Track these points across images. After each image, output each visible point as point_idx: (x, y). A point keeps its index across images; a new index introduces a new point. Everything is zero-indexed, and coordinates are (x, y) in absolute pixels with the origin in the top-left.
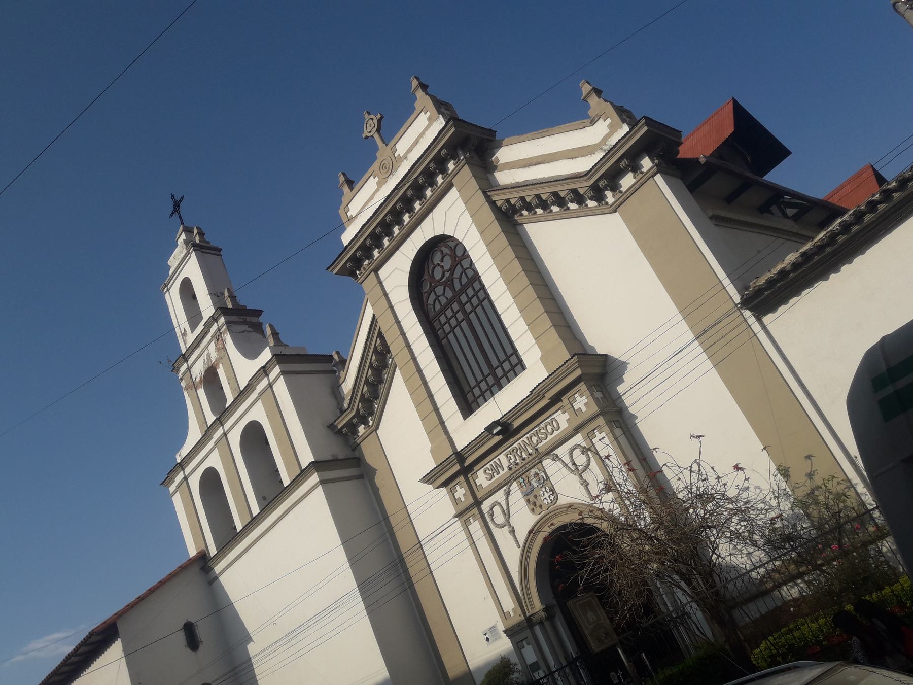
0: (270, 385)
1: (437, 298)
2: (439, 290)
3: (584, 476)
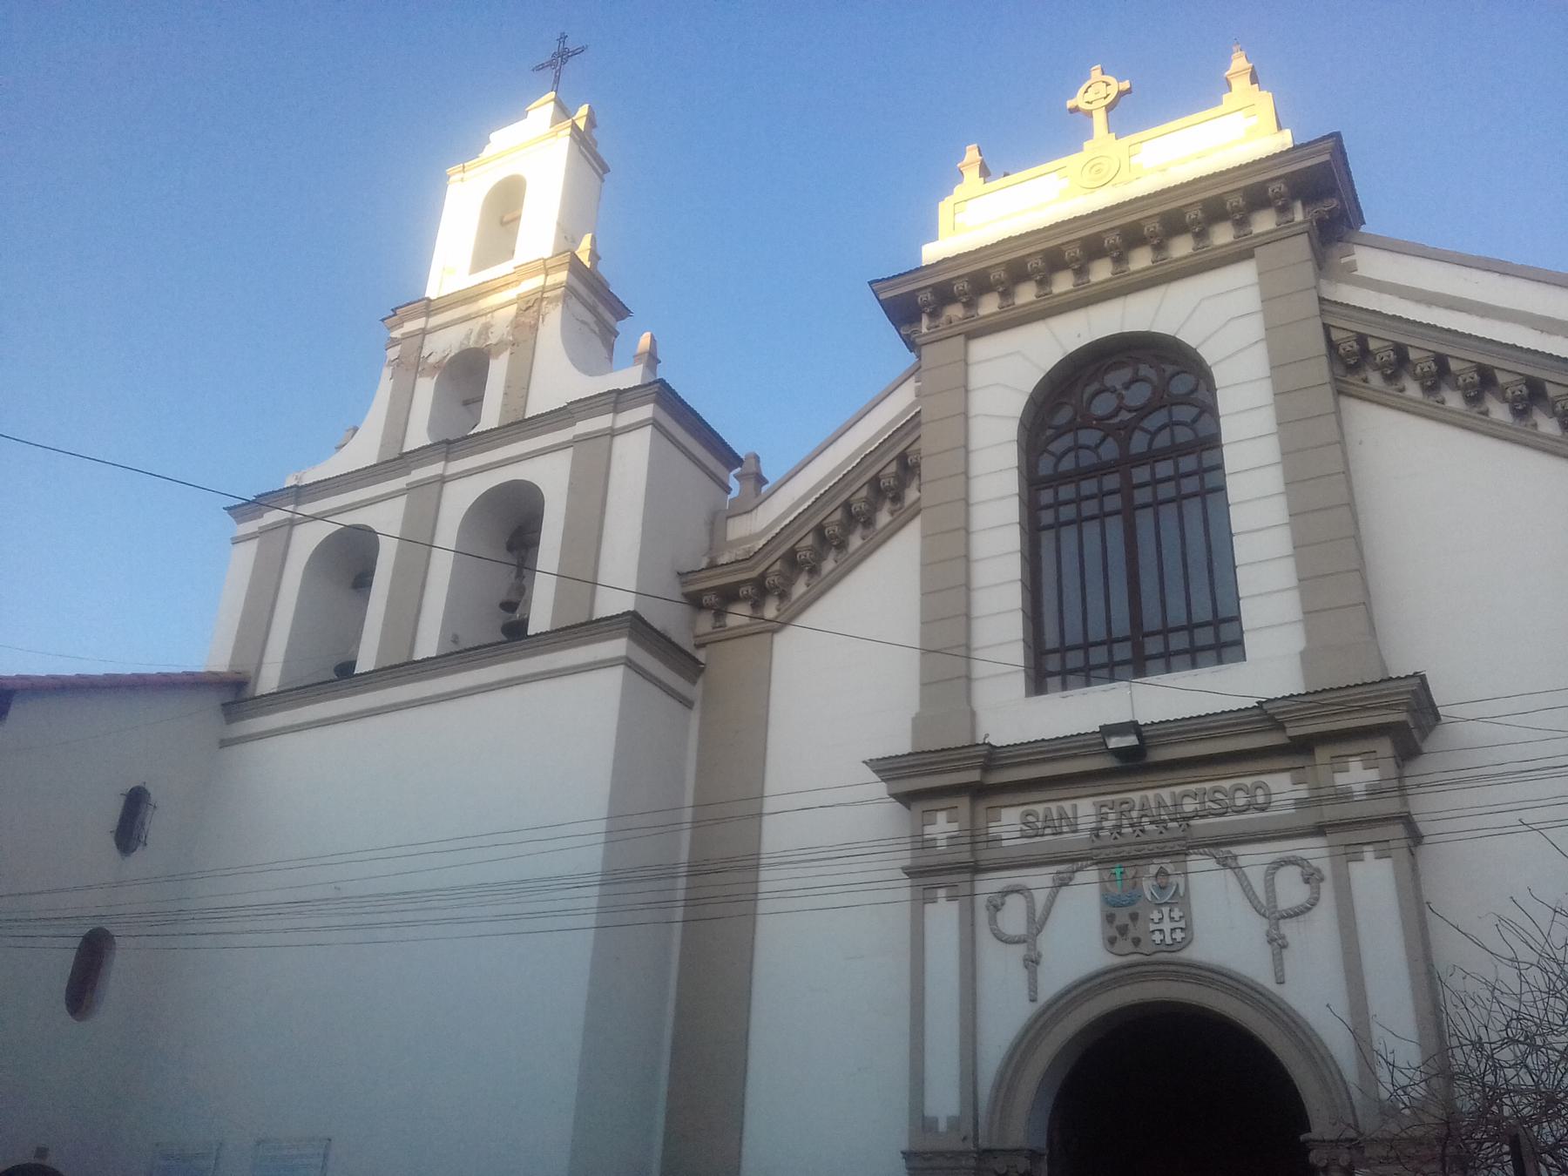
0: (612, 433)
1: (1077, 447)
2: (1089, 437)
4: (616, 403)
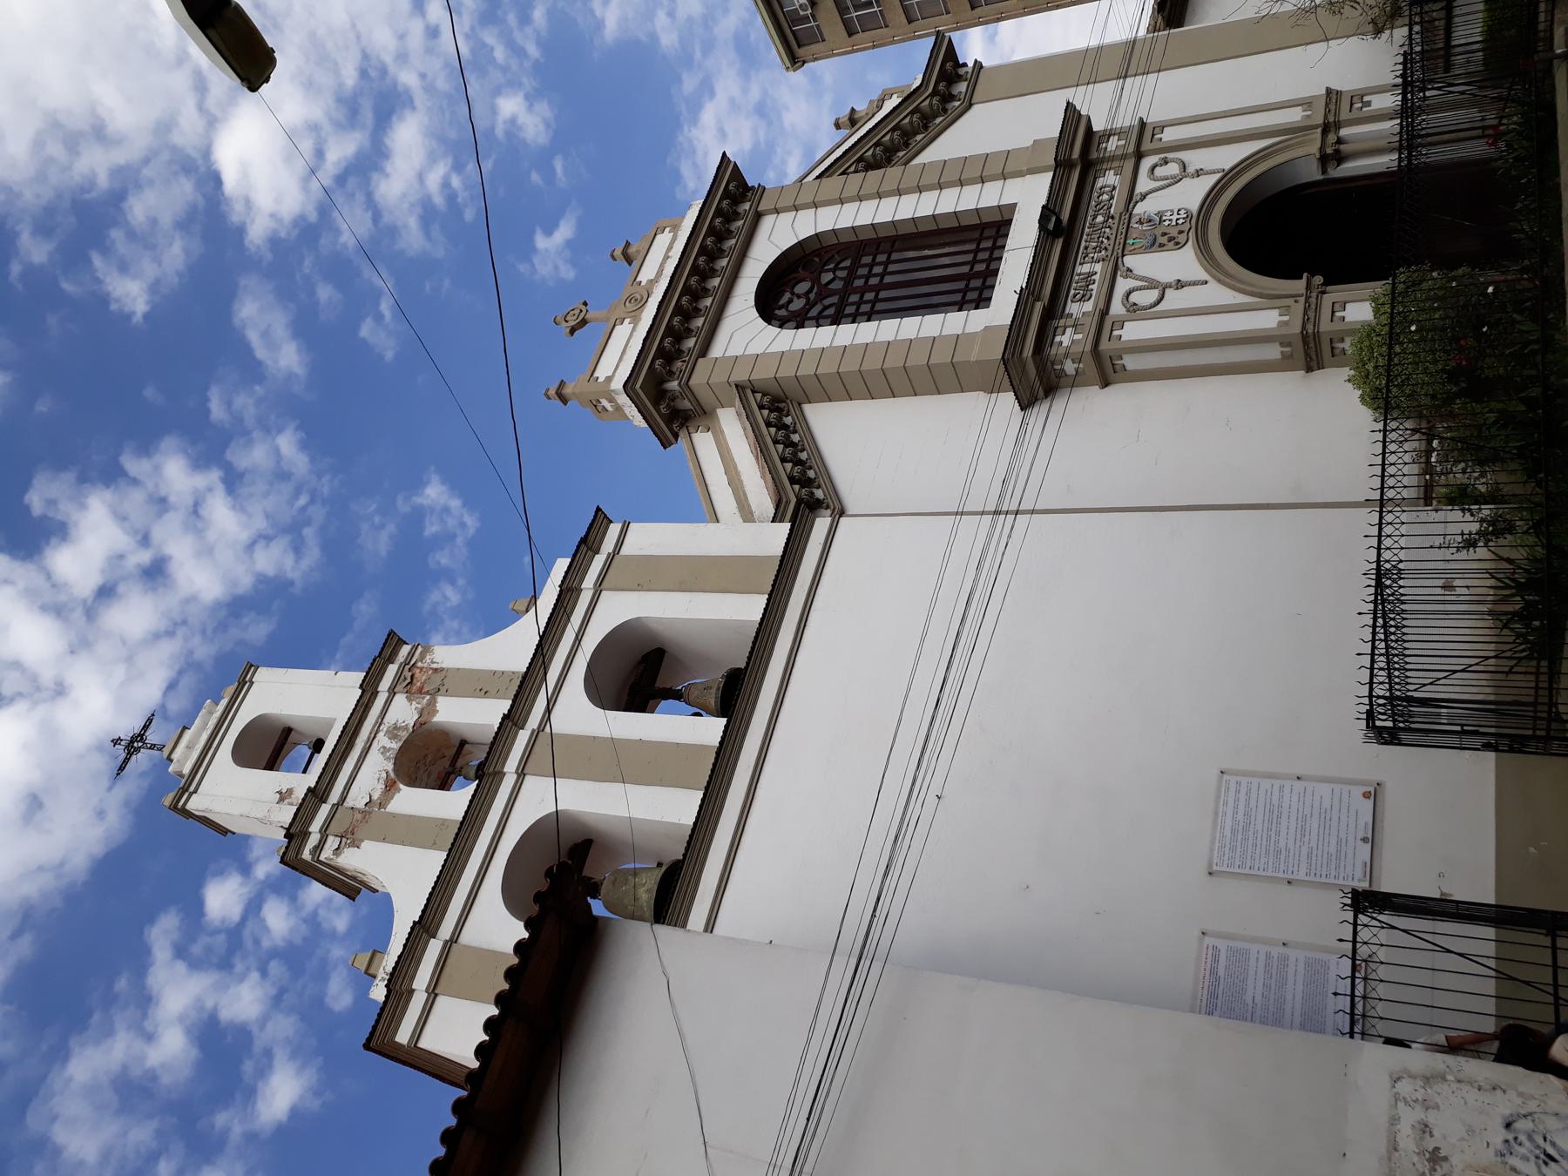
3: (1191, 169)
4: (589, 549)
